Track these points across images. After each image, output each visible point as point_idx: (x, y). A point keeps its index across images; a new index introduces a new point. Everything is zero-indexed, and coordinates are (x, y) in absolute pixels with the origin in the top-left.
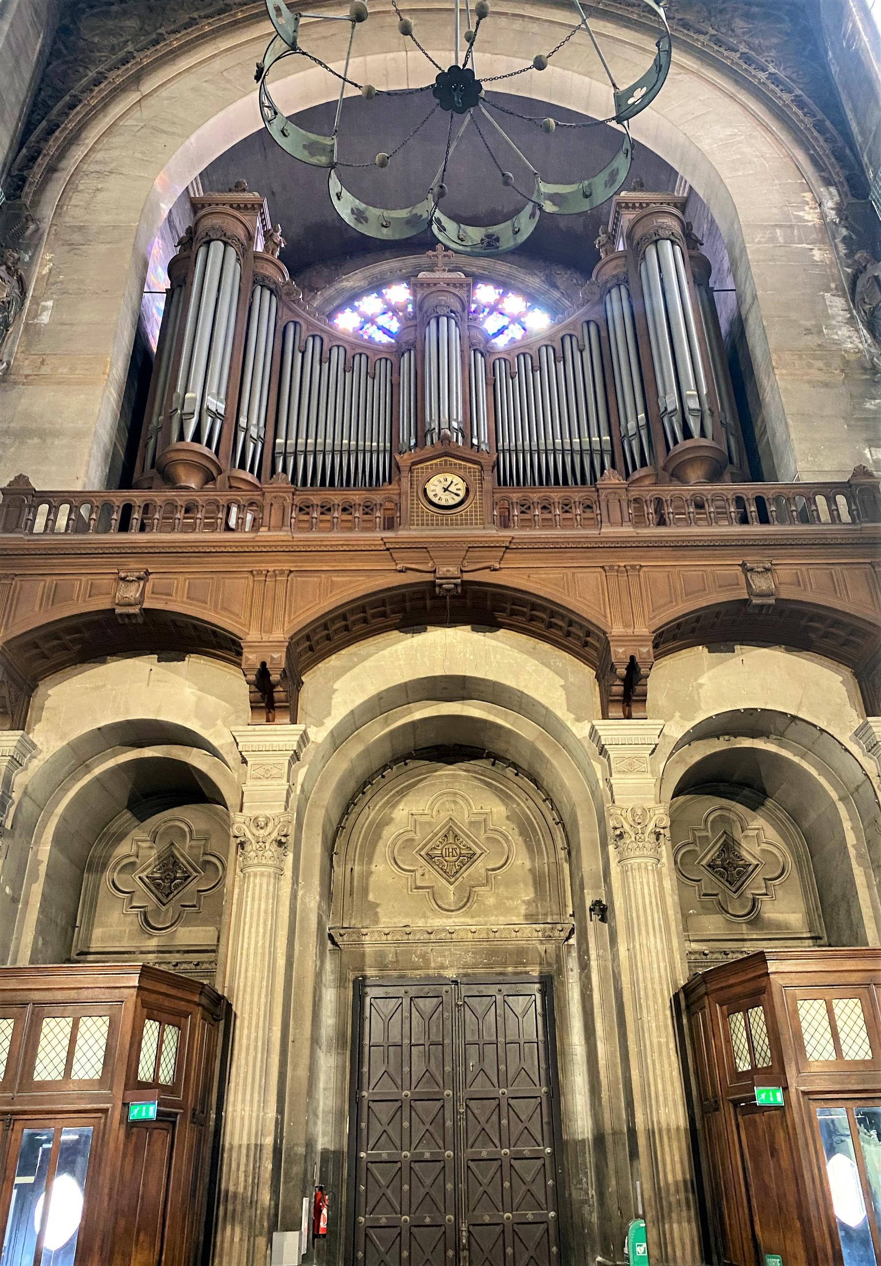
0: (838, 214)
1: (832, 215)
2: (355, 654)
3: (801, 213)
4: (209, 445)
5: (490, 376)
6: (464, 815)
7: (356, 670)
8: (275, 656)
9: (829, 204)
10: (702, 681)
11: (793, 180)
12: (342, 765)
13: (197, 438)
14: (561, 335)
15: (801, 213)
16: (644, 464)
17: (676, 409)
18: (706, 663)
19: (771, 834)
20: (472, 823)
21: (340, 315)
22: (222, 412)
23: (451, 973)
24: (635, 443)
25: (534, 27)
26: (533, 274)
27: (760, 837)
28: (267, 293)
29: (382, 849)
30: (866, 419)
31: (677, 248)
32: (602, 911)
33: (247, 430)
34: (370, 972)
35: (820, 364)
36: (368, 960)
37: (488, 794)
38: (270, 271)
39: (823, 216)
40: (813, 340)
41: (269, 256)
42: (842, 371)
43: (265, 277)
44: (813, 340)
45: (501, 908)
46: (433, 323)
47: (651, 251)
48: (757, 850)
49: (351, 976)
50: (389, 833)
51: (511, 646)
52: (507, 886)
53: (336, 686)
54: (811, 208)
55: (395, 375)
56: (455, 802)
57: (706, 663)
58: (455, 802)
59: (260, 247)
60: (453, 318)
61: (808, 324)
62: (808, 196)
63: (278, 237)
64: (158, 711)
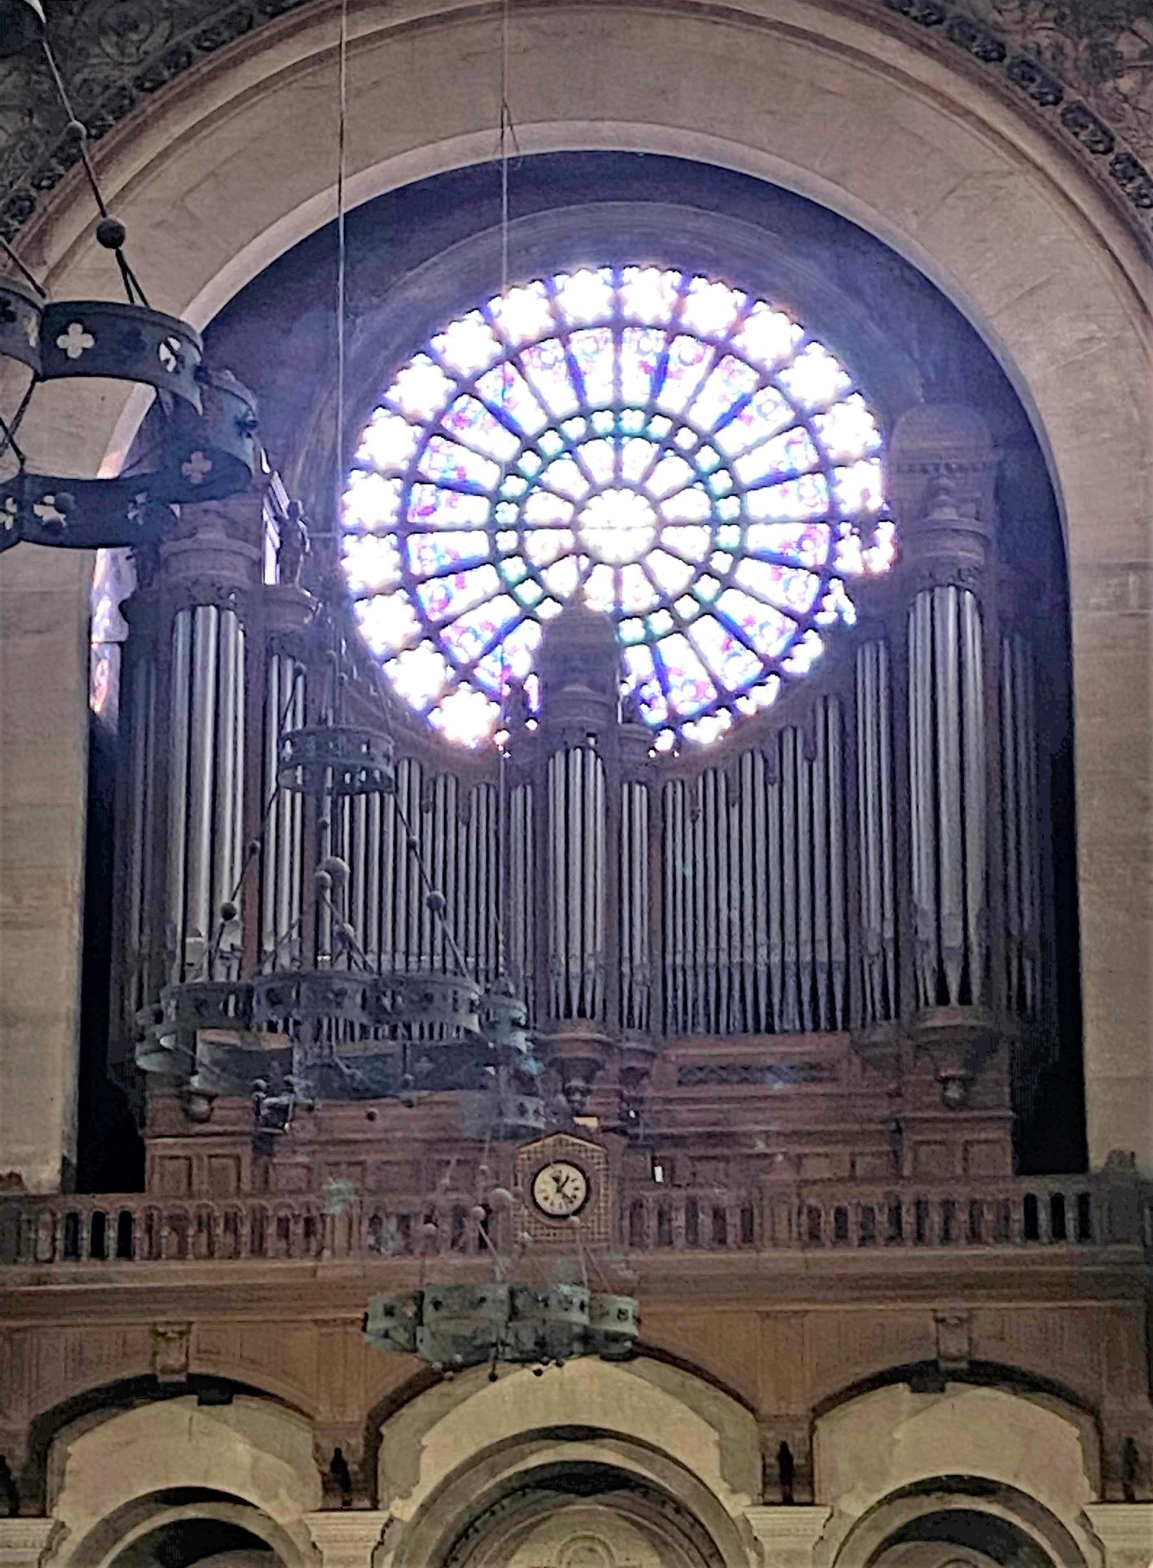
2: (448, 1395)
7: (451, 1417)
8: (353, 1442)
10: (898, 1436)
12: (435, 1535)
14: (781, 726)
16: (887, 1017)
18: (905, 1407)
21: (402, 376)
51: (650, 1381)
53: (424, 1441)
56: (592, 1550)
64: (206, 1475)
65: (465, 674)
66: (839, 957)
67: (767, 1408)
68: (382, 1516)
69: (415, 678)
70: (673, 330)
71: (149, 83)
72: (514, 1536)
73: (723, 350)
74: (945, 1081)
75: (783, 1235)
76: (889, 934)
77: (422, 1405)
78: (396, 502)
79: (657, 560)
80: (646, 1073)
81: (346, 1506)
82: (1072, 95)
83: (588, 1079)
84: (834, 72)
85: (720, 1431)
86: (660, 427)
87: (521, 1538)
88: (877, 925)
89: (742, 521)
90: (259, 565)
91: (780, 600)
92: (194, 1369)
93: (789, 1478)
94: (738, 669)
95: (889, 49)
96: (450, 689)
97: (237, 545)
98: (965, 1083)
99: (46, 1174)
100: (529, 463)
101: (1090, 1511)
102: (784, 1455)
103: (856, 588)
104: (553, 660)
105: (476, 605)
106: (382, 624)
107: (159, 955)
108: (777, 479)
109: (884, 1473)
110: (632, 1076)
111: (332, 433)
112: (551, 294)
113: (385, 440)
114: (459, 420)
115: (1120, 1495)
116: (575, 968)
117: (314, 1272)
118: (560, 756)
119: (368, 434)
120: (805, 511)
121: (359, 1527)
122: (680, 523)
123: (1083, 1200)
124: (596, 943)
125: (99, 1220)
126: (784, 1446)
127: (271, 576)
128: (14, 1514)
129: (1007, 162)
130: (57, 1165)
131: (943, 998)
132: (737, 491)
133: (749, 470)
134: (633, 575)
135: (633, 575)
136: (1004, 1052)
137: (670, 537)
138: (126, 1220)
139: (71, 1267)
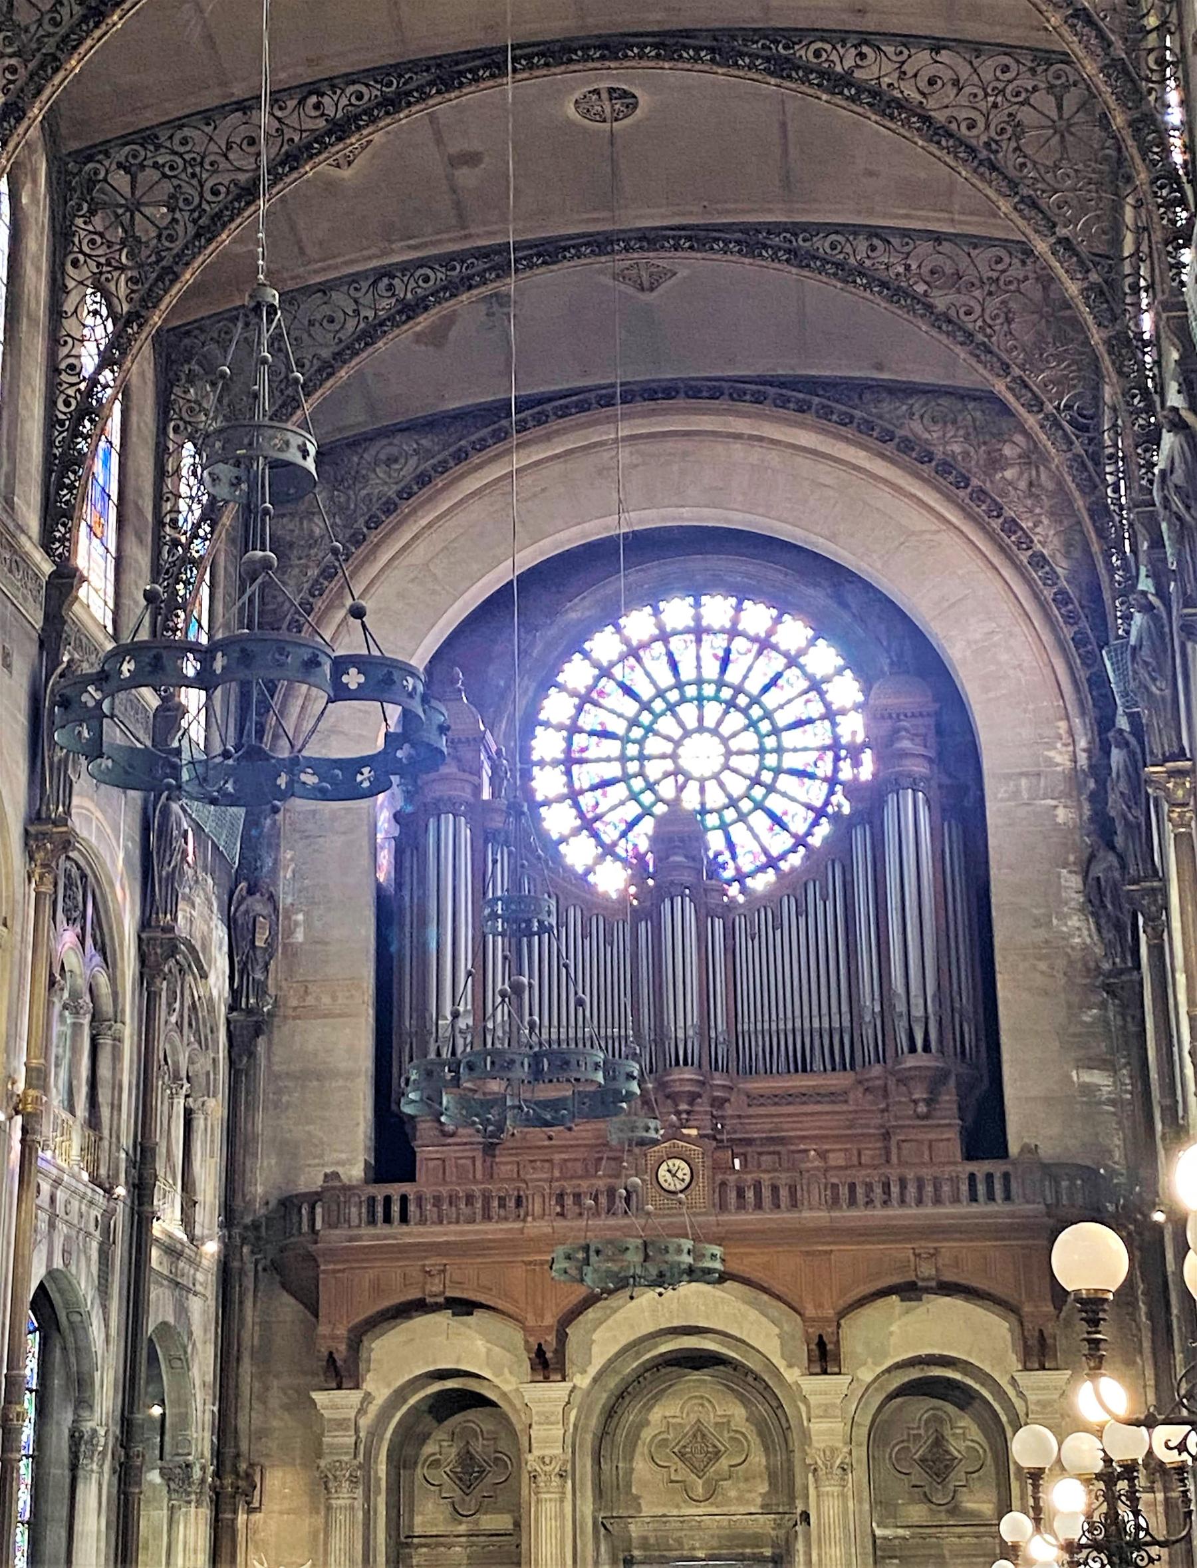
1: (1083, 759)
3: (1052, 754)
5: (730, 942)
6: (710, 1419)
7: (610, 1322)
8: (549, 1338)
9: (1083, 743)
10: (893, 1328)
11: (1048, 703)
15: (1052, 754)
18: (897, 1311)
19: (975, 1433)
20: (716, 1424)
21: (566, 666)
23: (701, 1554)
24: (870, 1031)
25: (774, 457)
26: (816, 585)
27: (965, 1435)
29: (641, 1449)
30: (1080, 1035)
32: (806, 1516)
34: (636, 1553)
35: (1042, 966)
36: (635, 1543)
37: (730, 1397)
40: (1041, 934)
44: (1041, 934)
45: (740, 1500)
48: (962, 1446)
49: (621, 1557)
50: (647, 1434)
52: (746, 1480)
56: (702, 1405)
57: (897, 1311)
58: (702, 1405)
62: (1063, 725)
65: (608, 850)
66: (846, 1023)
67: (810, 1312)
68: (568, 1385)
69: (578, 853)
70: (733, 632)
71: (406, 494)
72: (653, 1398)
73: (764, 644)
74: (915, 1102)
75: (815, 1202)
76: (877, 1009)
77: (591, 1314)
78: (564, 745)
79: (726, 776)
80: (728, 1100)
81: (546, 1379)
82: (975, 482)
83: (691, 1103)
84: (825, 473)
85: (781, 1328)
86: (726, 693)
87: (656, 1398)
88: (870, 1003)
89: (779, 750)
90: (478, 789)
91: (804, 799)
92: (448, 1294)
93: (824, 1357)
94: (779, 842)
95: (860, 457)
96: (600, 859)
97: (466, 776)
98: (929, 1102)
99: (356, 1172)
100: (646, 718)
101: (1017, 1376)
102: (821, 1344)
103: (853, 790)
104: (664, 841)
105: (615, 807)
106: (558, 820)
107: (422, 1032)
108: (799, 724)
109: (885, 1355)
110: (718, 1103)
111: (522, 704)
112: (657, 612)
113: (557, 707)
114: (601, 693)
115: (1036, 1366)
116: (681, 1035)
117: (521, 1231)
118: (668, 902)
119: (546, 703)
120: (818, 743)
121: (555, 1392)
122: (741, 753)
123: (1006, 1177)
124: (694, 1017)
125: (388, 1200)
126: (820, 1337)
127: (486, 795)
128: (339, 1388)
129: (935, 525)
130: (362, 1165)
131: (913, 1049)
132: (776, 731)
133: (782, 719)
134: (711, 786)
135: (711, 786)
136: (952, 1082)
137: (735, 761)
138: (404, 1199)
139: (372, 1231)
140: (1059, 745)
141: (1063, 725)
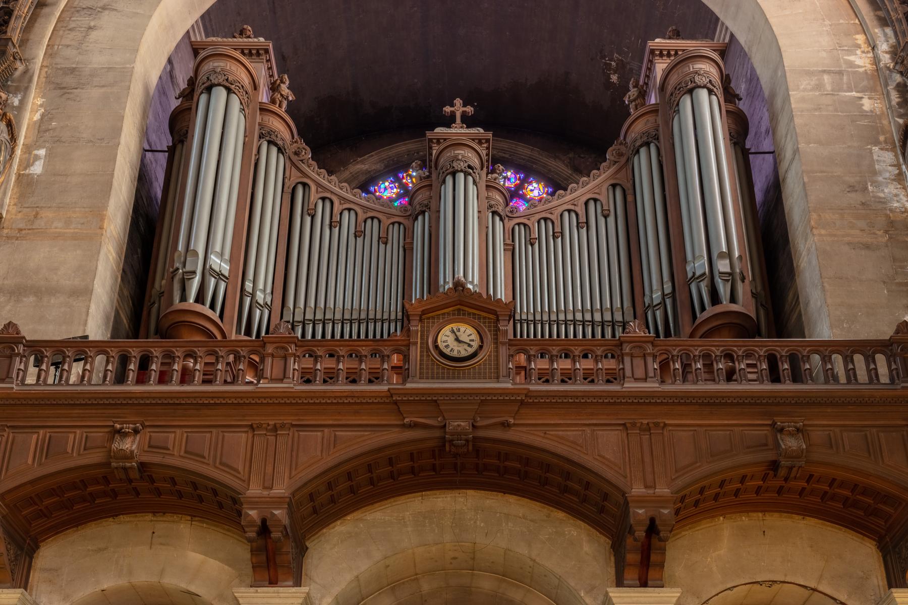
0: (893, 59)
1: (886, 59)
3: (852, 58)
4: (212, 307)
9: (883, 47)
13: (200, 298)
15: (852, 58)
17: (704, 274)
22: (227, 274)
28: (274, 150)
31: (714, 98)
33: (253, 295)
35: (862, 224)
38: (276, 125)
39: (876, 60)
40: (855, 198)
41: (275, 108)
42: (886, 232)
43: (271, 132)
44: (855, 198)
46: (449, 180)
47: (686, 102)
54: (863, 52)
55: (408, 240)
59: (264, 96)
60: (470, 174)
61: (851, 180)
63: (285, 89)
76: (668, 288)
140: (859, 52)
141: (860, 38)
